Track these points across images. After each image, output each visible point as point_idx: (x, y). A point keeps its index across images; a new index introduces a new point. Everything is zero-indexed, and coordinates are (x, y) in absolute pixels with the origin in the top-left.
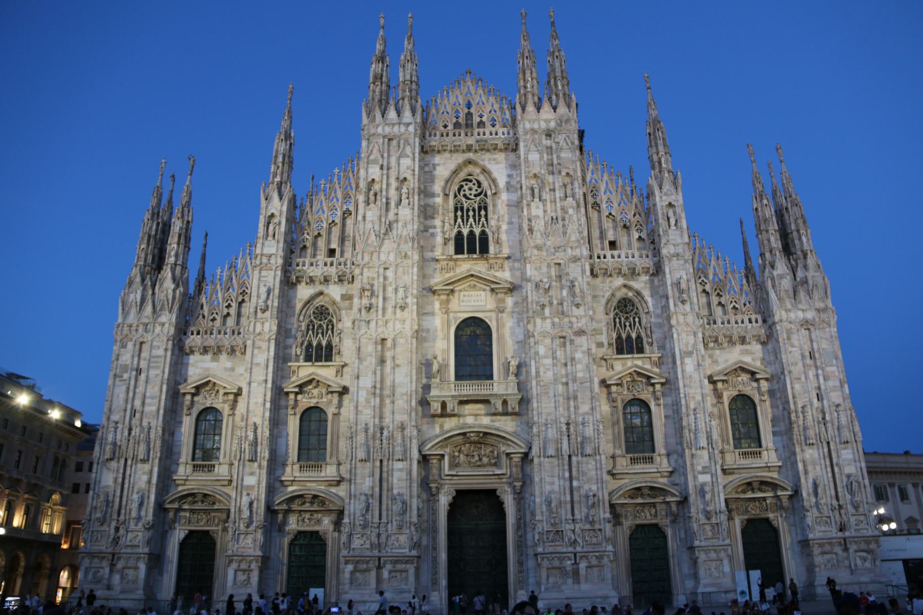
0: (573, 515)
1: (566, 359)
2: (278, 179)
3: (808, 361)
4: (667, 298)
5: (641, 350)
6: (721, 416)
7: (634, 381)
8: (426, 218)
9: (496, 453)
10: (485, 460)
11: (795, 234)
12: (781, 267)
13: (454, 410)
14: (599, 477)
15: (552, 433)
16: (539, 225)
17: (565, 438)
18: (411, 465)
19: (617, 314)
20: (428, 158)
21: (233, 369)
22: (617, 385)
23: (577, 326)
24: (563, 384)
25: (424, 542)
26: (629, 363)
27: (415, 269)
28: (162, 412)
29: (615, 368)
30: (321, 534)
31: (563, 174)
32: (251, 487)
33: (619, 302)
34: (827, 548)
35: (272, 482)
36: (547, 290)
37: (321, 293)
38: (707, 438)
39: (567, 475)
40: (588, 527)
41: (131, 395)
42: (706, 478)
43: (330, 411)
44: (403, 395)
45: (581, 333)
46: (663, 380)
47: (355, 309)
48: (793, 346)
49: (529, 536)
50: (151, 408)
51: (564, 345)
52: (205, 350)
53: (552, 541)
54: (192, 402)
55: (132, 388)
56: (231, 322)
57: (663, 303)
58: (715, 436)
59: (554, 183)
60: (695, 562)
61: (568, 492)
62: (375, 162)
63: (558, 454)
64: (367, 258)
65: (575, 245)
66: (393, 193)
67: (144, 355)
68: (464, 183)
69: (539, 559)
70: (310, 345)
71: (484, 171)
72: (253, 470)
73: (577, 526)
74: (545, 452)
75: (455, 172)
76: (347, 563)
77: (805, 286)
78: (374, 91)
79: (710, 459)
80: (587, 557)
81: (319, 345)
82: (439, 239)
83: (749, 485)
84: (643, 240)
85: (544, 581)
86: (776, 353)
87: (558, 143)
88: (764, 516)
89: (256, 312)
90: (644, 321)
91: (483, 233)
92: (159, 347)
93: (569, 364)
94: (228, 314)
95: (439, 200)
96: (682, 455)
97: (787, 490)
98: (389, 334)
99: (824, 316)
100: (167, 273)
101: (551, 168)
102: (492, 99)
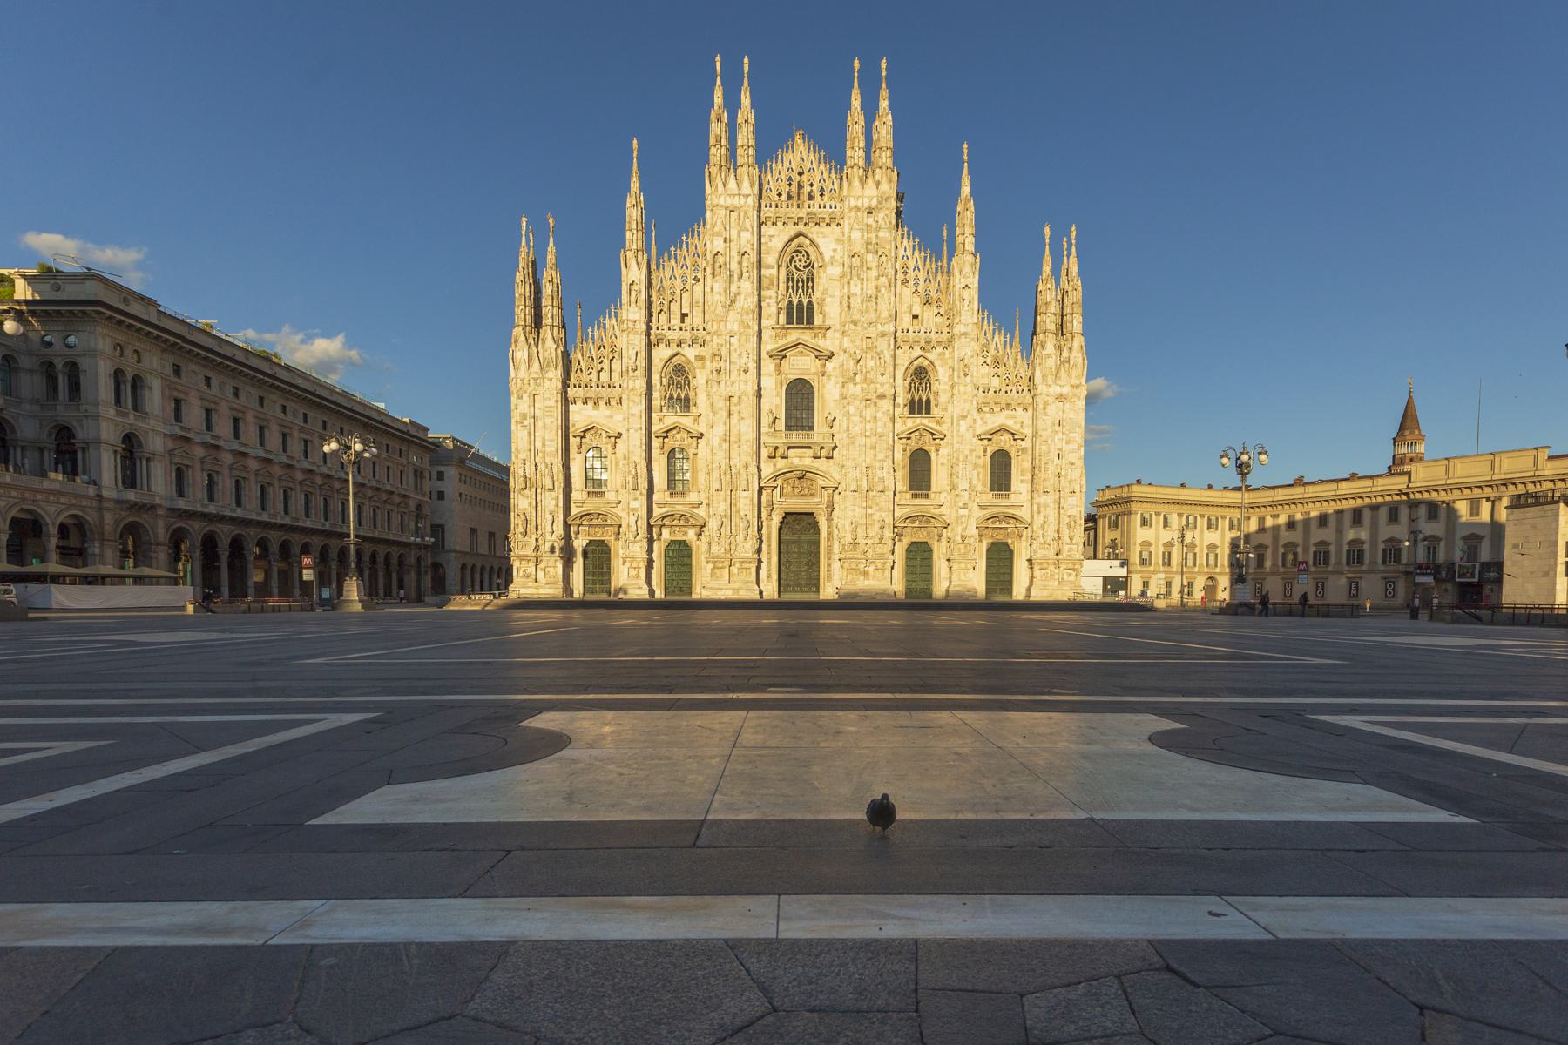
3: (1056, 428)
23: (880, 391)
32: (635, 510)
43: (691, 451)
45: (882, 397)
52: (586, 402)
56: (604, 377)
66: (734, 266)
71: (813, 243)
75: (787, 244)
82: (774, 309)
91: (810, 303)
95: (774, 272)
98: (735, 391)
99: (1077, 391)
100: (546, 333)
102: (822, 166)
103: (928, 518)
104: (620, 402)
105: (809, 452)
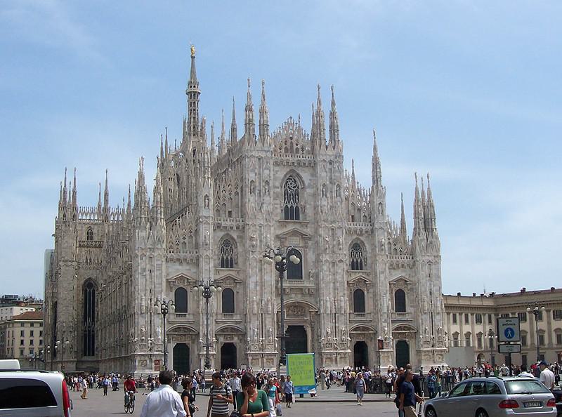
3: (428, 278)
4: (375, 247)
5: (361, 269)
6: (392, 298)
12: (423, 235)
26: (357, 275)
34: (427, 353)
47: (247, 245)
51: (334, 266)
62: (253, 171)
70: (223, 258)
71: (298, 175)
75: (285, 176)
82: (279, 211)
95: (279, 190)
96: (376, 313)
99: (437, 259)
103: (365, 329)
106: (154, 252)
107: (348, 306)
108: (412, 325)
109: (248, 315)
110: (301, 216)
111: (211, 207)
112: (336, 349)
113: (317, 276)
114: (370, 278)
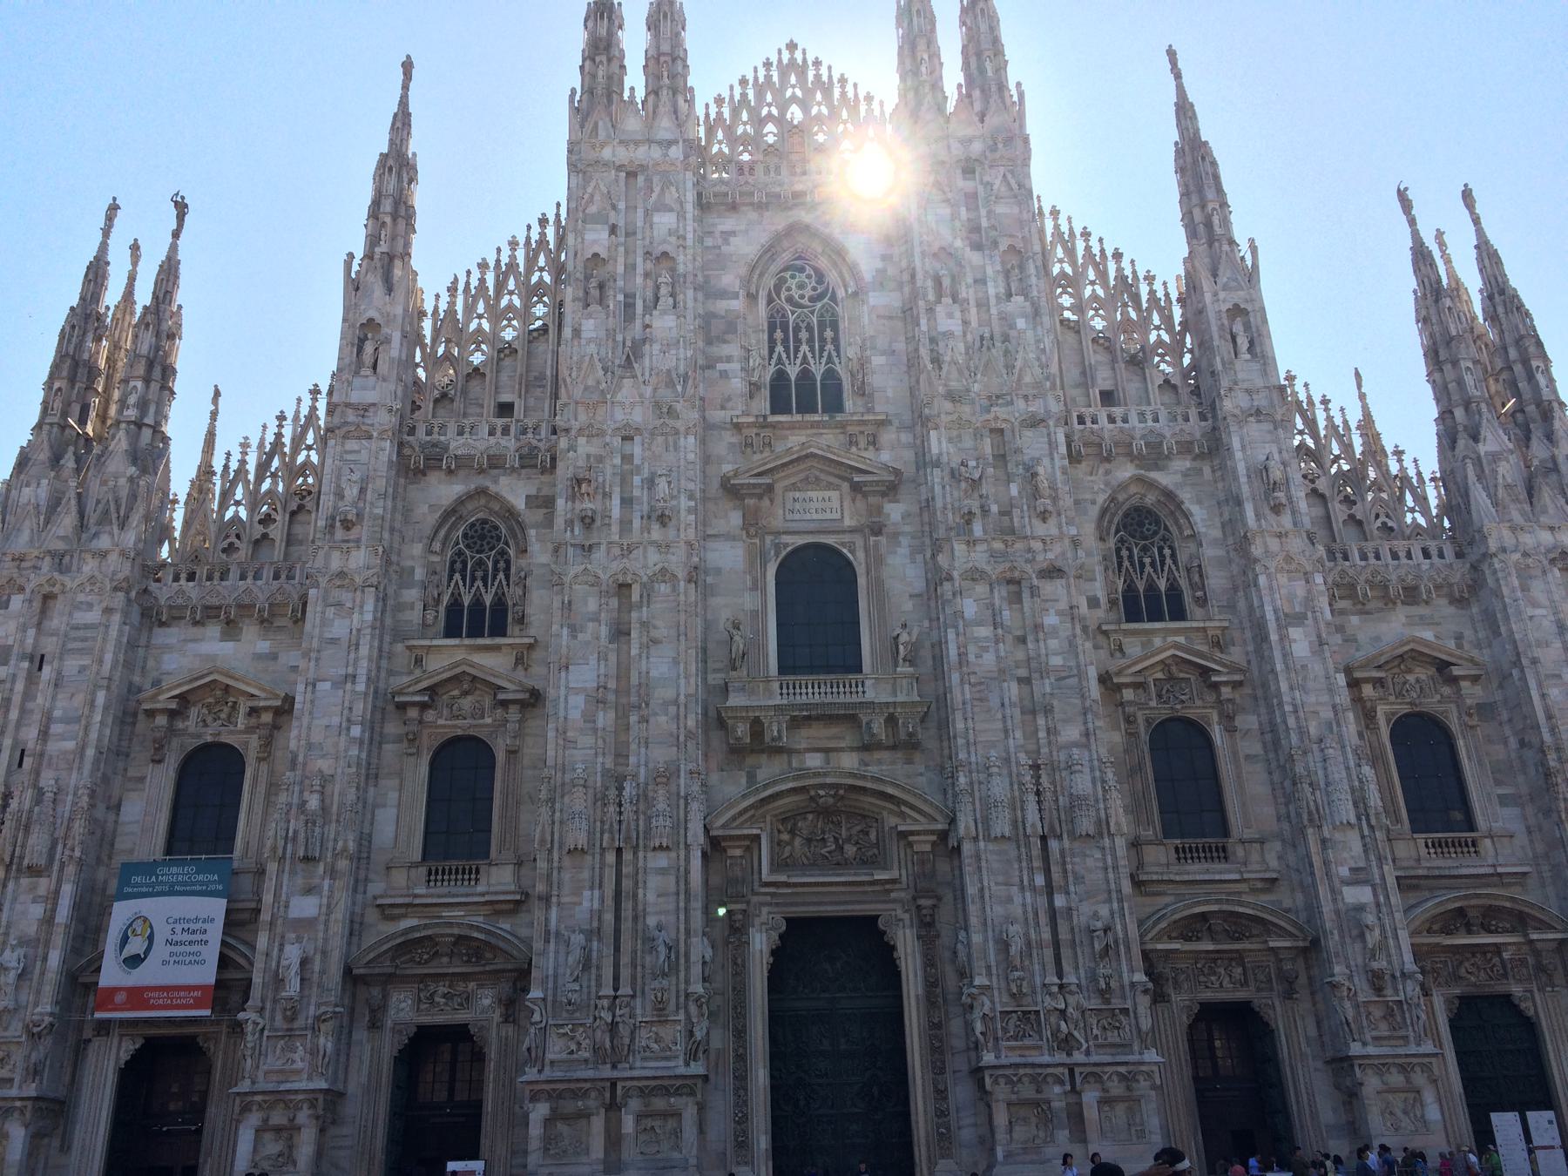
0: (1060, 975)
1: (1024, 627)
2: (383, 247)
4: (1239, 503)
6: (1376, 760)
7: (1171, 678)
8: (709, 342)
9: (873, 836)
10: (850, 850)
11: (1518, 368)
12: (1494, 440)
13: (780, 737)
14: (1113, 886)
15: (999, 788)
16: (955, 351)
17: (1032, 798)
18: (687, 860)
19: (1122, 541)
20: (711, 219)
21: (274, 657)
22: (1136, 686)
24: (1020, 680)
25: (716, 1043)
26: (1158, 642)
27: (691, 439)
28: (90, 752)
29: (1128, 650)
30: (473, 1030)
31: (1003, 247)
33: (1126, 515)
35: (358, 909)
36: (975, 484)
37: (482, 492)
38: (1355, 804)
39: (1040, 880)
40: (1095, 1003)
41: (14, 715)
42: (1363, 895)
44: (666, 704)
45: (1053, 572)
46: (1237, 677)
47: (559, 522)
48: (1535, 605)
49: (956, 1025)
50: (63, 745)
51: (1016, 599)
53: (1015, 1038)
54: (171, 731)
55: (17, 699)
57: (1226, 516)
58: (1374, 799)
59: (984, 267)
60: (1351, 1096)
61: (1043, 919)
62: (599, 218)
63: (1018, 835)
64: (583, 417)
65: (1031, 392)
67: (56, 622)
68: (788, 275)
69: (988, 1081)
72: (316, 881)
73: (1072, 1000)
74: (987, 828)
75: (770, 252)
76: (534, 1098)
77: (1554, 477)
78: (594, 76)
79: (1366, 851)
80: (1098, 1077)
81: (477, 603)
82: (737, 384)
83: (1458, 919)
84: (1174, 387)
85: (1001, 1136)
86: (1491, 622)
87: (989, 185)
88: (1500, 988)
89: (332, 526)
90: (1182, 558)
92: (90, 606)
93: (1030, 638)
94: (265, 536)
96: (1295, 839)
97: (1551, 928)
101: (975, 237)
103: (1239, 925)
104: (299, 617)
105: (849, 739)
106: (68, 570)
107: (1115, 794)
108: (1531, 896)
109: (542, 865)
110: (848, 404)
111: (382, 367)
112: (1066, 1043)
113: (939, 659)
114: (1236, 655)
